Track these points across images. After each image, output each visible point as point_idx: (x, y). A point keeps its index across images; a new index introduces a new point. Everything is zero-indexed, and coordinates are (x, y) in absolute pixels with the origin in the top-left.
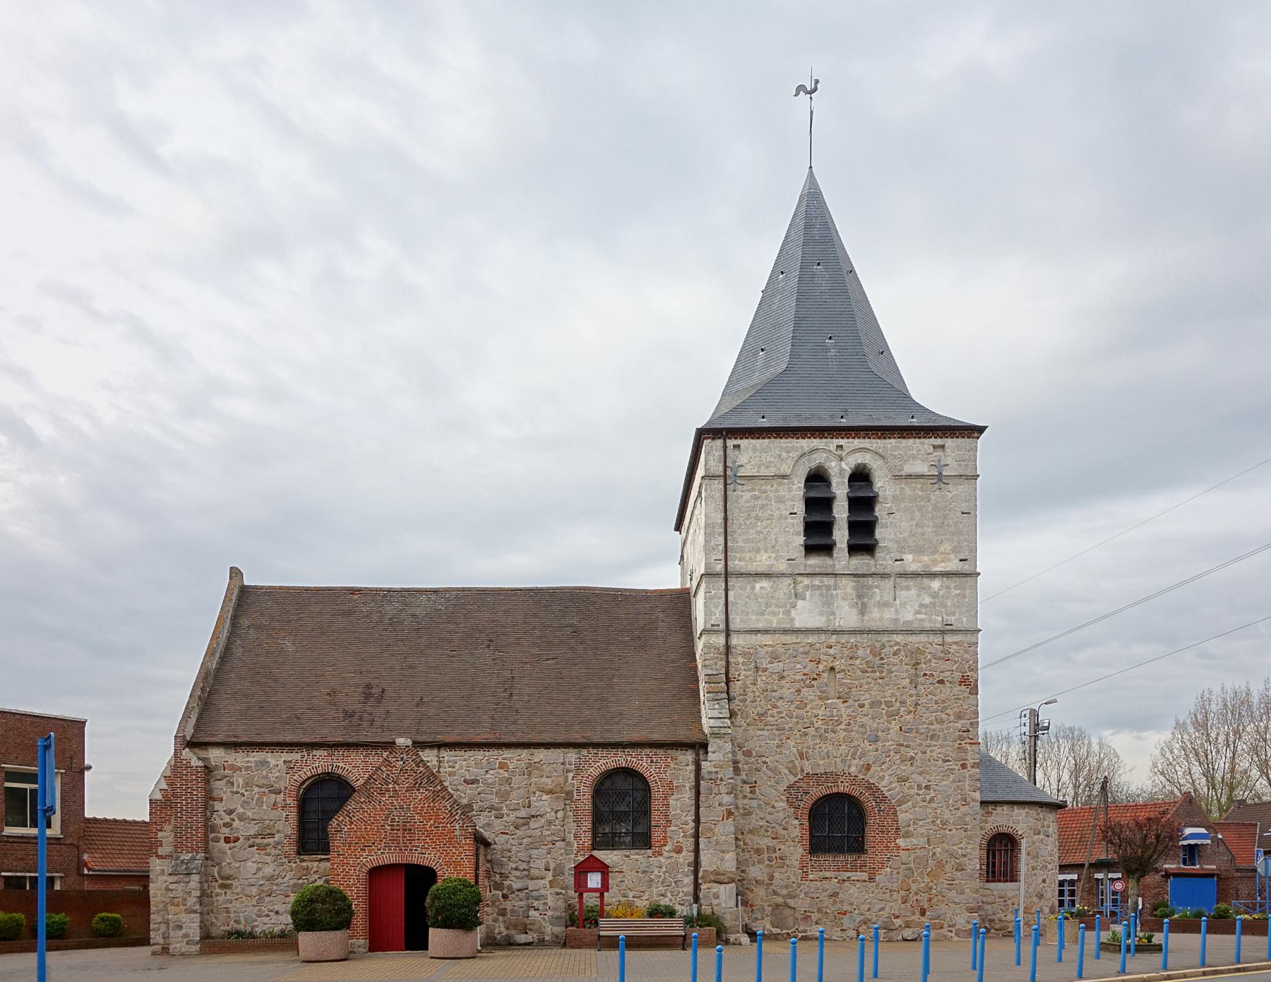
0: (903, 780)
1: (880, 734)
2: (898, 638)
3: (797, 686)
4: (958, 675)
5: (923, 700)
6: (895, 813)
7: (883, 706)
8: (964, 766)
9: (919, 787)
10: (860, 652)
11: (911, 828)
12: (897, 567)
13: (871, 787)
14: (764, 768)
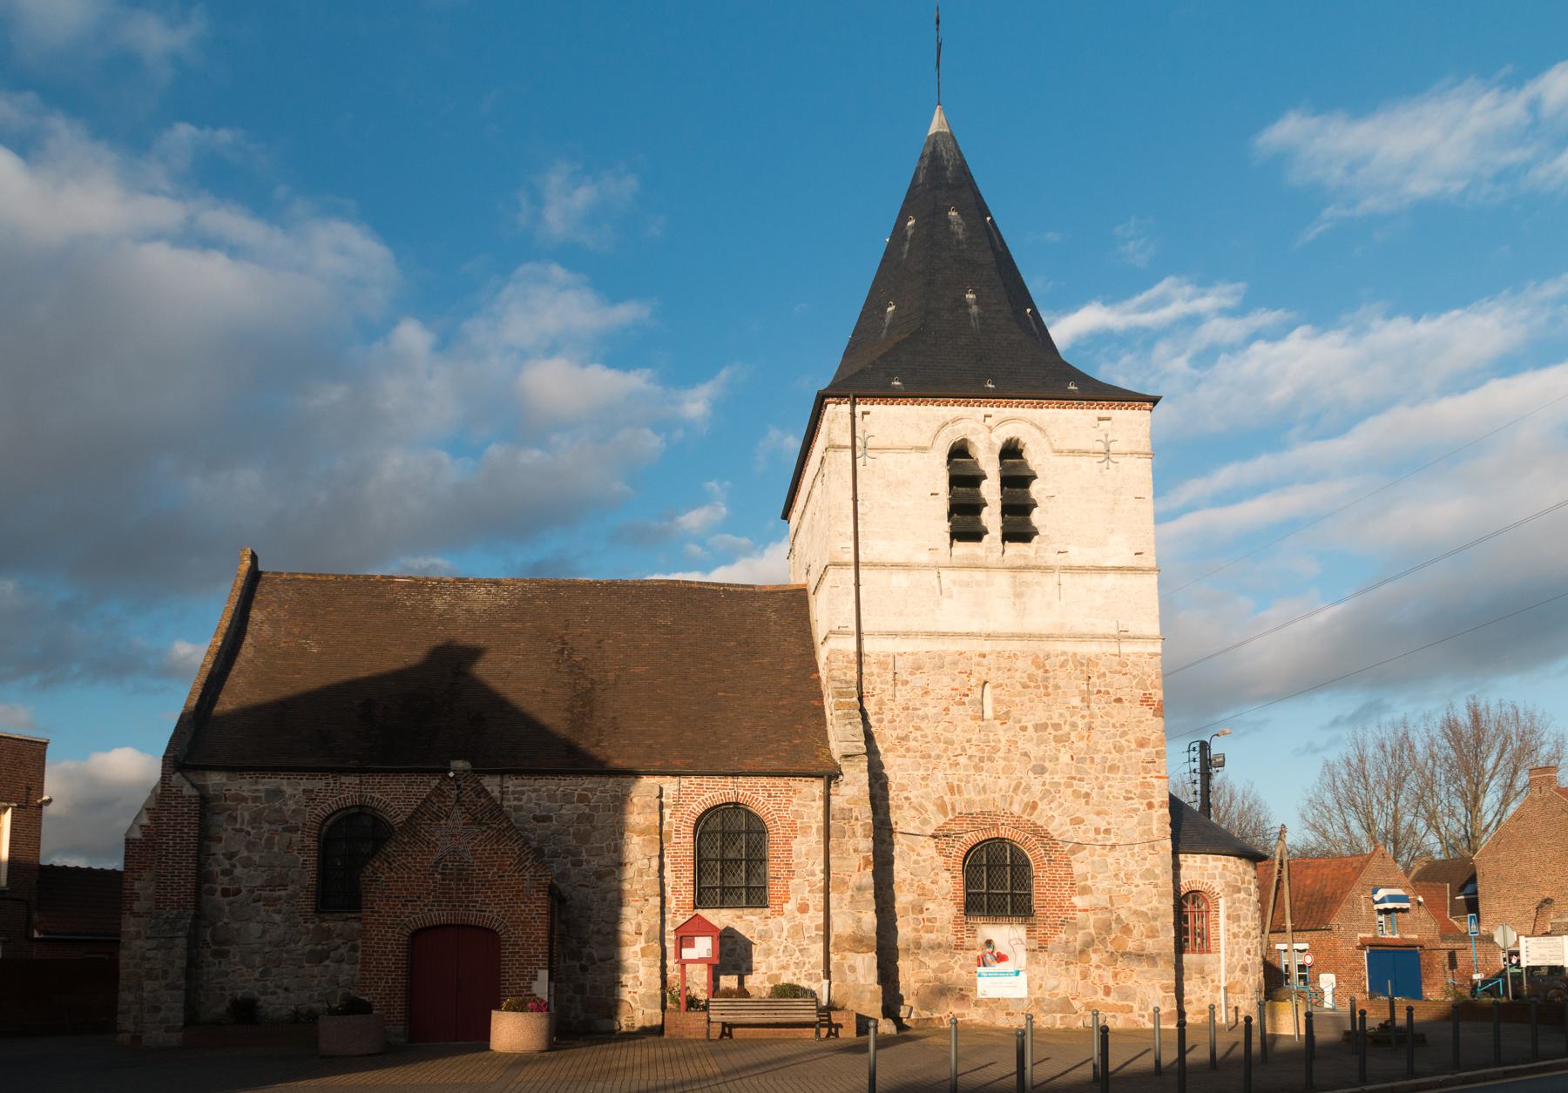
0: (1077, 821)
1: (1047, 764)
2: (1060, 647)
3: (944, 704)
5: (1097, 723)
6: (1069, 865)
7: (1050, 729)
8: (1150, 806)
9: (1097, 831)
10: (1020, 664)
11: (1089, 883)
12: (1062, 560)
13: (1040, 834)
14: (906, 805)
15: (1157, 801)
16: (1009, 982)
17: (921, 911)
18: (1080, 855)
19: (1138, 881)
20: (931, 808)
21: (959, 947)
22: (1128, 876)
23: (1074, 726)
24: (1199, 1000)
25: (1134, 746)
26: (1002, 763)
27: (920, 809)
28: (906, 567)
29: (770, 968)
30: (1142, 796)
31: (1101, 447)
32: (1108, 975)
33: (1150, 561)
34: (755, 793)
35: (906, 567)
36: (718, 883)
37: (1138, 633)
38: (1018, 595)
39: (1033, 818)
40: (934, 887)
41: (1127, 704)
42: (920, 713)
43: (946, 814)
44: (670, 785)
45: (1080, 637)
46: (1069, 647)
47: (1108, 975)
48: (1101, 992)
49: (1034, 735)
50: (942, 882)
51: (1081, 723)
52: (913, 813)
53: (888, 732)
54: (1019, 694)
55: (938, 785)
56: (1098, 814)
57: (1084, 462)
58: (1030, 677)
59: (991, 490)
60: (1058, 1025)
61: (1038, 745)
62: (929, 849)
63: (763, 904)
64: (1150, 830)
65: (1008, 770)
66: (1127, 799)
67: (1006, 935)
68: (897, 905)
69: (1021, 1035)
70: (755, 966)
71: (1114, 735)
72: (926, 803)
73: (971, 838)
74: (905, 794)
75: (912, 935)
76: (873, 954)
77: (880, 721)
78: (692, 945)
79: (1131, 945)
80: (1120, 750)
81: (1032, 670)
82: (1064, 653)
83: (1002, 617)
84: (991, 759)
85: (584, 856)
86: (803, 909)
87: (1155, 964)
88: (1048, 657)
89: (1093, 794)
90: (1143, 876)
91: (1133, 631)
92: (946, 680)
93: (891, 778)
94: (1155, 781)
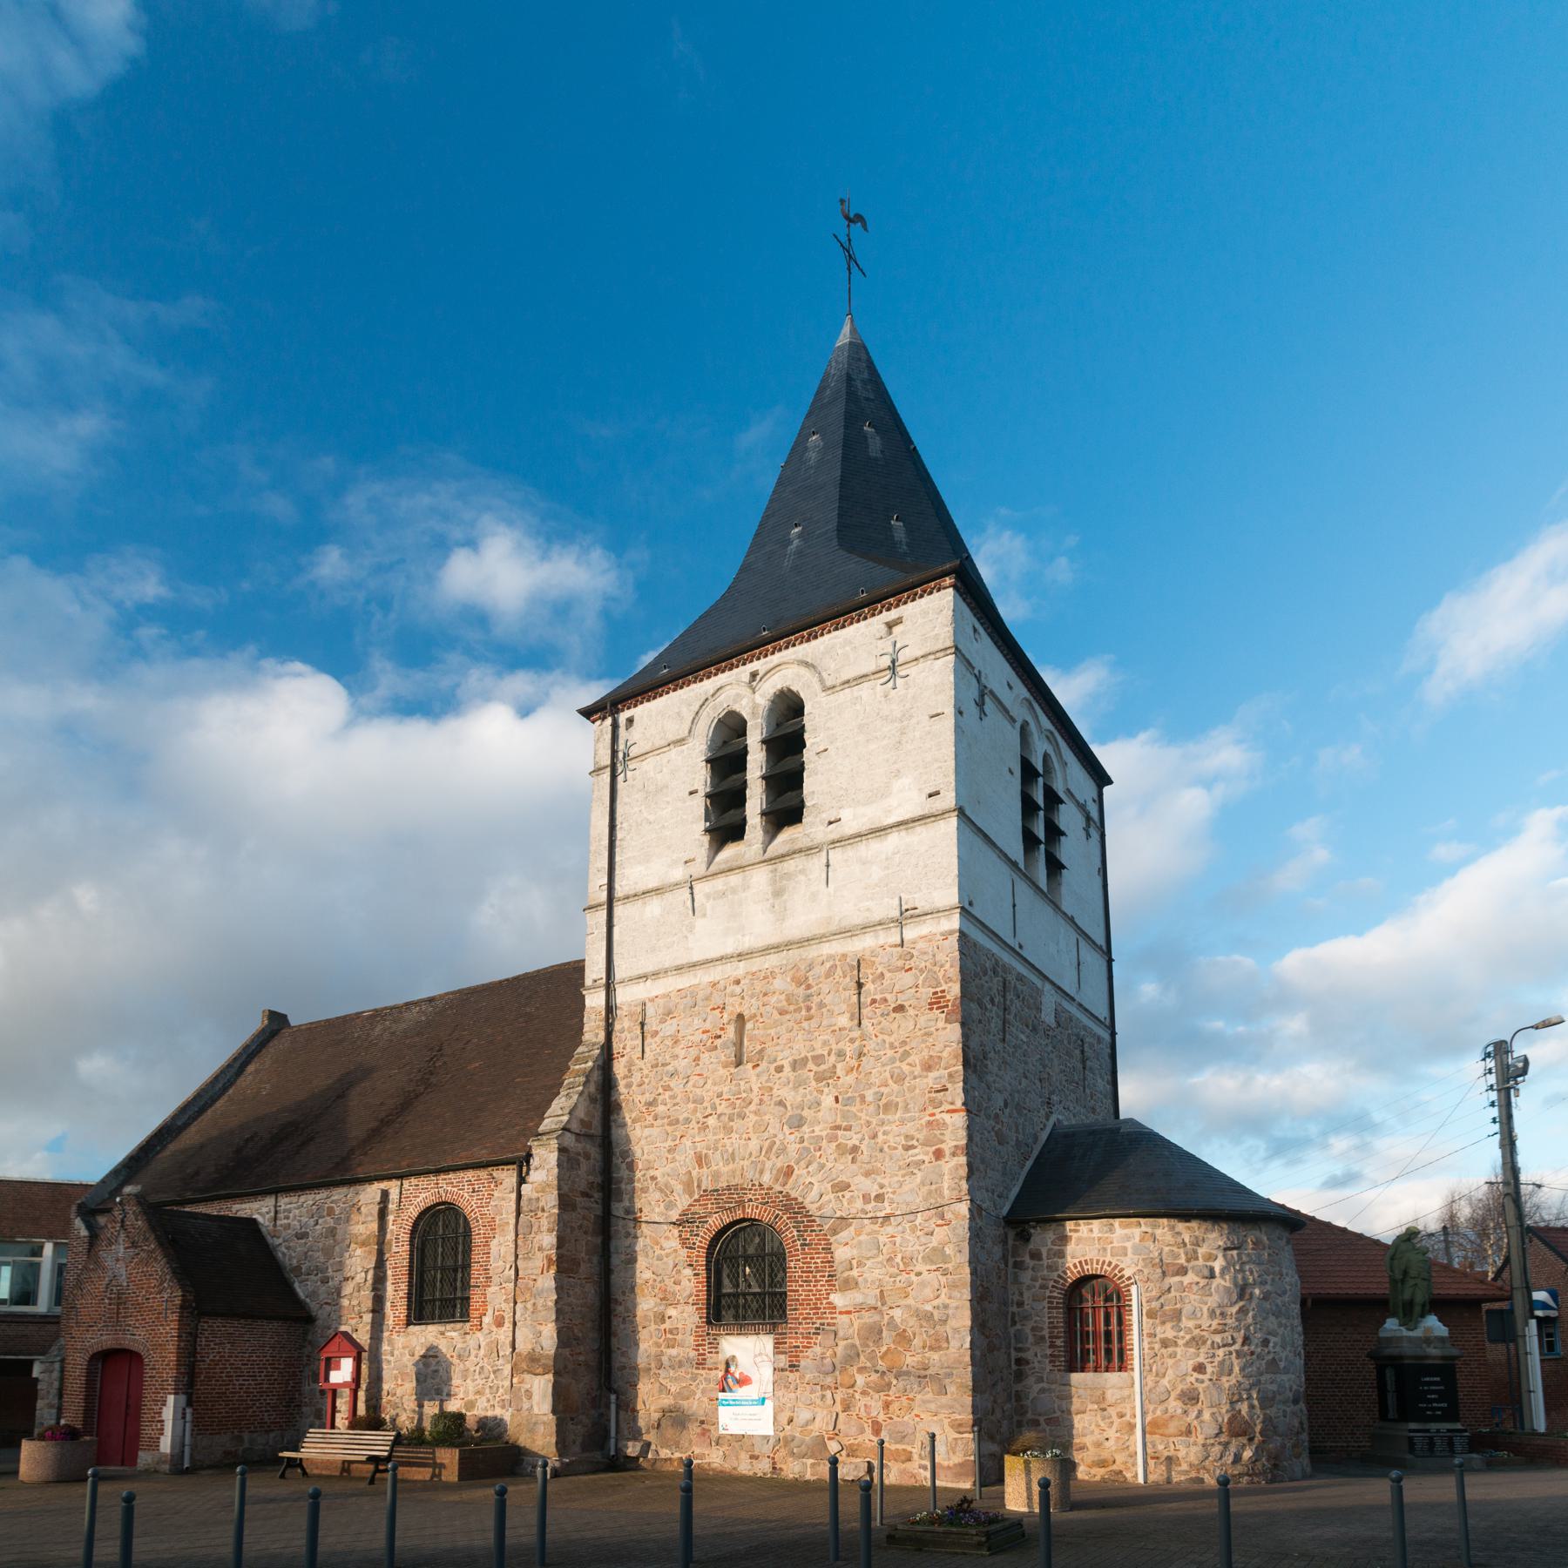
1: (806, 1113)
2: (828, 949)
3: (693, 1052)
4: (926, 993)
5: (870, 1045)
6: (828, 1250)
7: (811, 1065)
8: (939, 1154)
9: (866, 1198)
10: (778, 984)
11: (855, 1273)
12: (834, 832)
13: (794, 1208)
14: (652, 1187)
15: (947, 1147)
16: (743, 1408)
17: (663, 1321)
18: (844, 1235)
19: (920, 1267)
20: (679, 1188)
21: (701, 1364)
22: (908, 1261)
23: (841, 1054)
24: (1098, 1445)
25: (917, 1071)
26: (753, 1118)
27: (666, 1191)
28: (657, 891)
29: (466, 1392)
30: (926, 1143)
31: (886, 661)
32: (875, 1403)
33: (948, 799)
34: (457, 1188)
35: (657, 891)
36: (438, 1295)
37: (927, 908)
38: (778, 893)
39: (787, 1189)
40: (677, 1288)
41: (911, 1012)
42: (670, 1068)
43: (691, 1194)
44: (393, 1187)
45: (848, 932)
46: (828, 949)
47: (875, 1403)
48: (869, 1430)
49: (792, 1075)
50: (685, 1282)
51: (849, 1049)
52: (657, 1195)
53: (638, 1098)
54: (776, 1024)
55: (685, 1157)
56: (867, 1174)
57: (864, 690)
58: (789, 999)
59: (756, 762)
60: (808, 1477)
61: (795, 1088)
62: (671, 1241)
63: (465, 1317)
64: (939, 1191)
65: (762, 1127)
66: (908, 1148)
67: (750, 1351)
68: (639, 1313)
69: (867, 1487)
70: (454, 1391)
71: (893, 1060)
72: (673, 1182)
73: (716, 1222)
74: (652, 1172)
75: (654, 1350)
76: (550, 1377)
77: (629, 1086)
78: (338, 1368)
79: (910, 1360)
80: (899, 1079)
81: (792, 988)
82: (831, 957)
83: (760, 928)
84: (742, 1117)
85: (330, 1273)
86: (499, 1323)
87: (943, 1391)
88: (810, 967)
89: (863, 1147)
90: (928, 1259)
91: (923, 906)
92: (697, 1022)
93: (638, 1154)
94: (946, 1117)
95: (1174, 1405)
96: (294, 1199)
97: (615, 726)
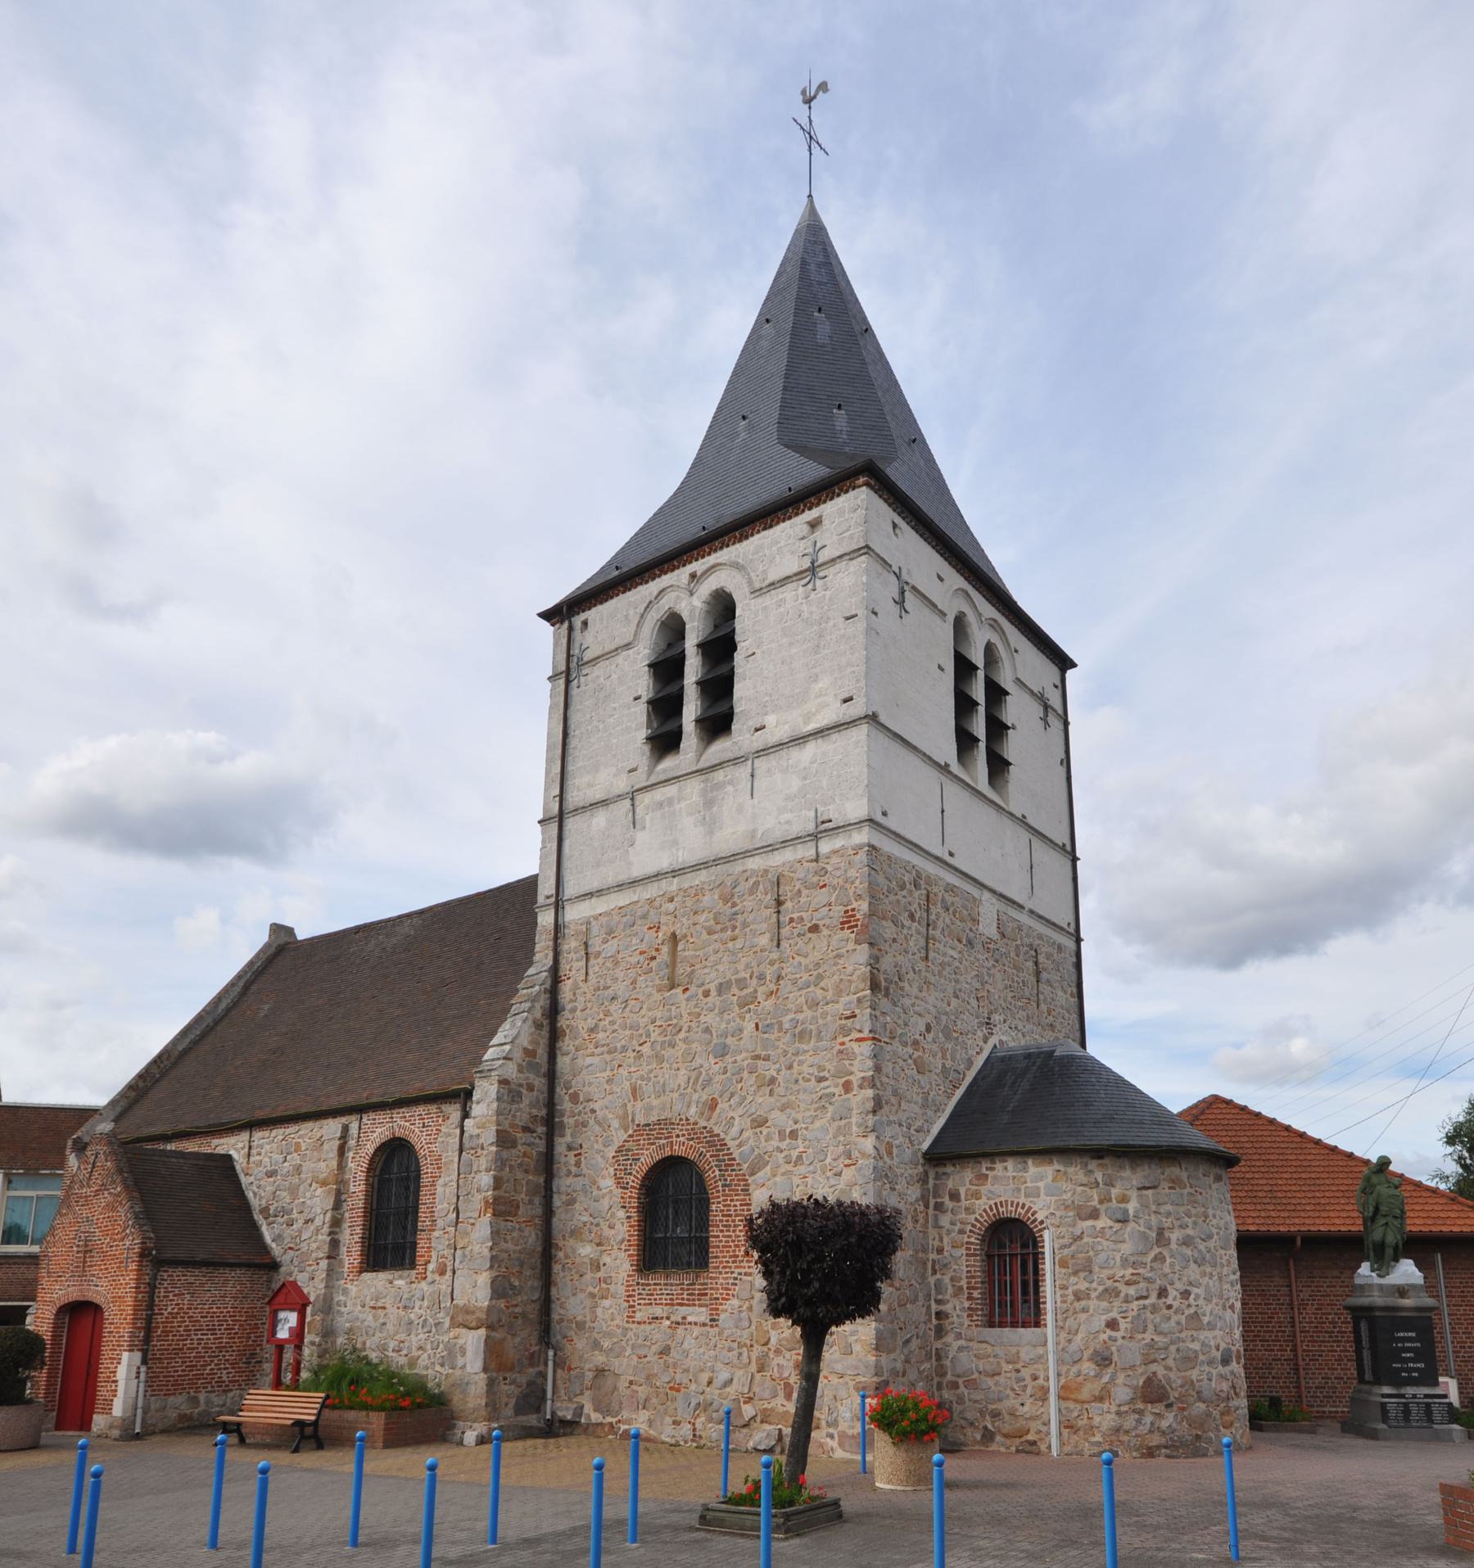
0: (760, 1123)
1: (729, 1041)
2: (754, 864)
3: (632, 973)
4: (838, 910)
5: (788, 969)
7: (734, 990)
8: (847, 1087)
9: (782, 1135)
10: (706, 900)
13: (716, 1144)
15: (855, 1079)
17: (598, 1269)
20: (615, 1124)
23: (761, 977)
26: (682, 1046)
34: (409, 1124)
38: (709, 803)
40: (613, 1232)
41: (825, 932)
42: (610, 992)
45: (771, 848)
50: (618, 1226)
56: (783, 1109)
65: (690, 1056)
66: (821, 1080)
77: (574, 1010)
83: (692, 844)
84: (673, 1045)
89: (780, 1078)
94: (855, 1045)
95: (1088, 1368)
96: (266, 1133)
97: (571, 629)
